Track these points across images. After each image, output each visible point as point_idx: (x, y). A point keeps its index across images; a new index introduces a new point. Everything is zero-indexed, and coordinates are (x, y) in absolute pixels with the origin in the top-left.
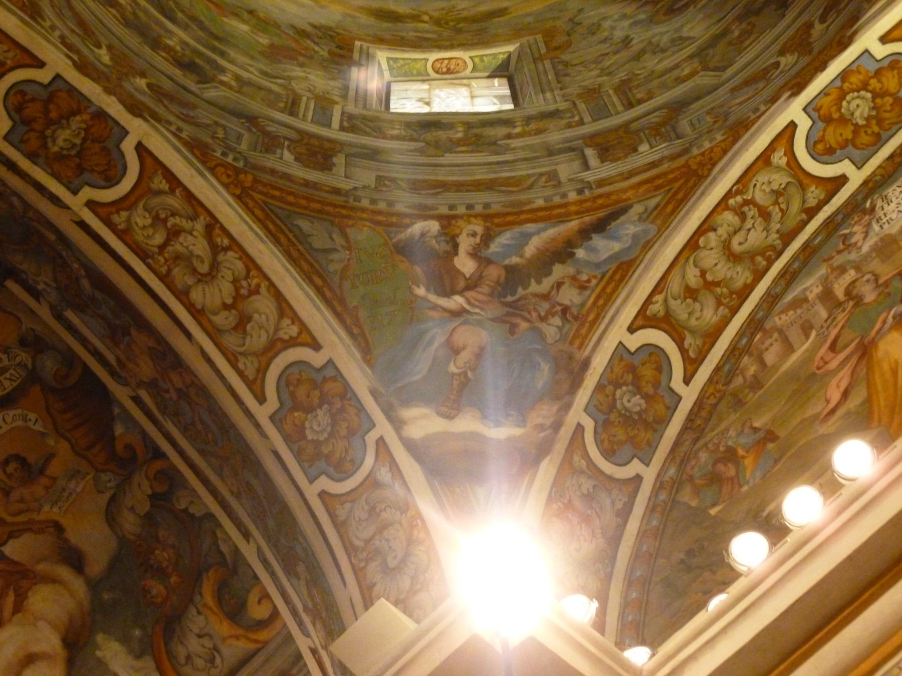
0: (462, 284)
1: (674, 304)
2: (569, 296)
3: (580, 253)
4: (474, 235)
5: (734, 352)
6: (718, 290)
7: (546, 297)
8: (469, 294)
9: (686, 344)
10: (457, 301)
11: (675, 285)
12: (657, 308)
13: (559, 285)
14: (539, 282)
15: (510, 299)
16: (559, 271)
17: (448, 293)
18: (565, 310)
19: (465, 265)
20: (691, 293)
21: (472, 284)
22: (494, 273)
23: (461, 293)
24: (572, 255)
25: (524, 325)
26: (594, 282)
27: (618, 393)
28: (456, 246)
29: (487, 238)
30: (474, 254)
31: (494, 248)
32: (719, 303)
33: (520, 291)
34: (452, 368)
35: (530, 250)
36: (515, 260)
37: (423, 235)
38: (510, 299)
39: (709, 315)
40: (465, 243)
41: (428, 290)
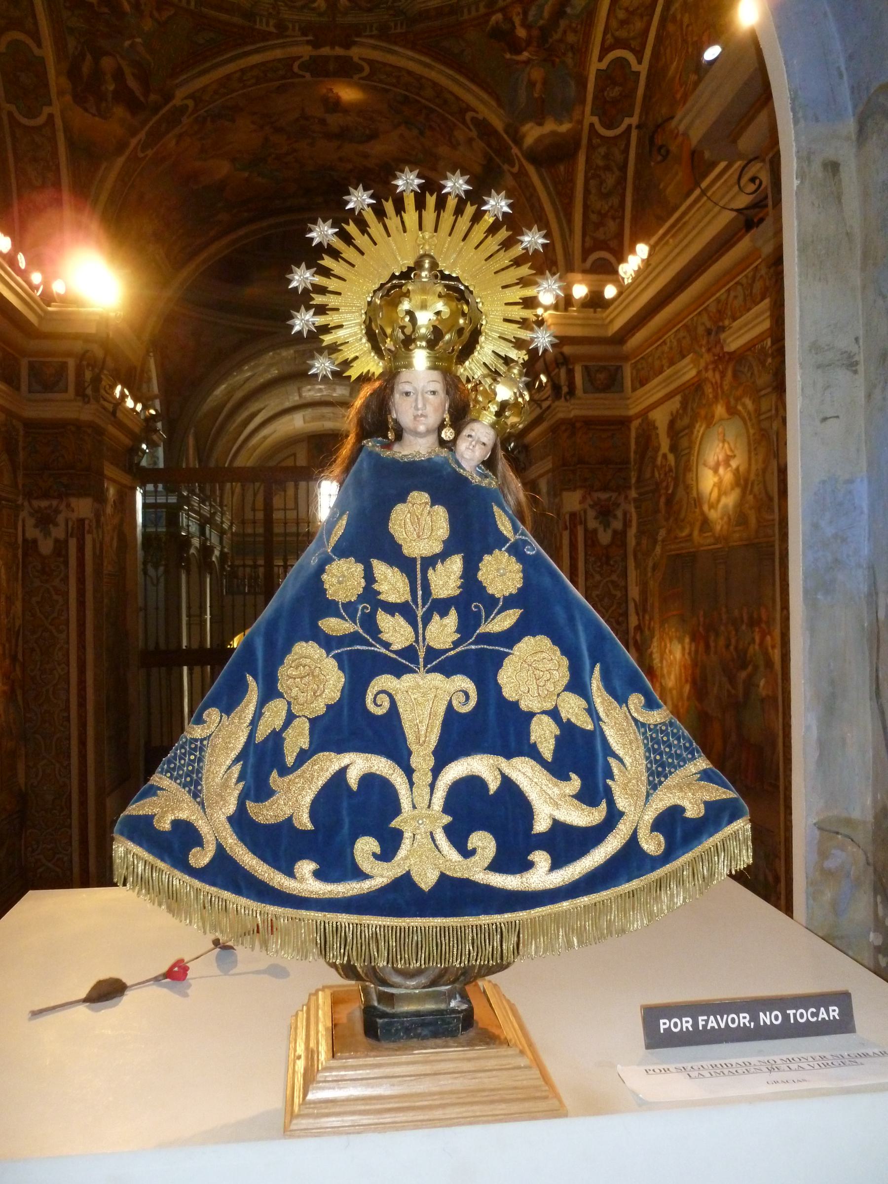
0: (524, 45)
1: (617, 34)
2: (571, 38)
3: (569, 10)
4: (519, 14)
5: (659, 39)
6: (639, 11)
7: (561, 41)
8: (531, 49)
9: (633, 46)
10: (525, 55)
11: (614, 24)
12: (610, 40)
13: (565, 32)
14: (556, 32)
15: (547, 46)
16: (563, 23)
17: (519, 52)
18: (572, 47)
19: (521, 33)
20: (623, 23)
21: (529, 42)
22: (535, 33)
23: (525, 50)
24: (565, 12)
25: (557, 60)
26: (579, 27)
27: (606, 94)
28: (513, 24)
29: (525, 13)
30: (524, 24)
31: (530, 18)
32: (642, 16)
33: (550, 40)
34: (536, 95)
35: (546, 14)
36: (541, 22)
37: (497, 23)
38: (547, 46)
39: (639, 25)
40: (517, 20)
41: (511, 53)
